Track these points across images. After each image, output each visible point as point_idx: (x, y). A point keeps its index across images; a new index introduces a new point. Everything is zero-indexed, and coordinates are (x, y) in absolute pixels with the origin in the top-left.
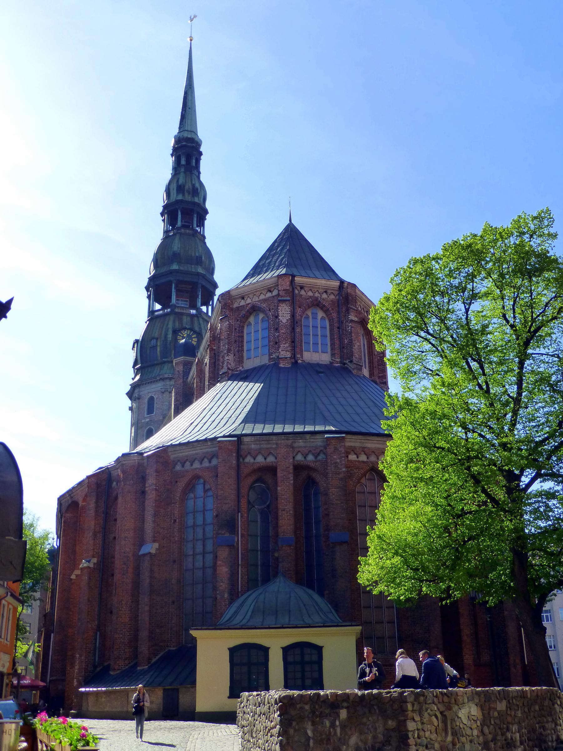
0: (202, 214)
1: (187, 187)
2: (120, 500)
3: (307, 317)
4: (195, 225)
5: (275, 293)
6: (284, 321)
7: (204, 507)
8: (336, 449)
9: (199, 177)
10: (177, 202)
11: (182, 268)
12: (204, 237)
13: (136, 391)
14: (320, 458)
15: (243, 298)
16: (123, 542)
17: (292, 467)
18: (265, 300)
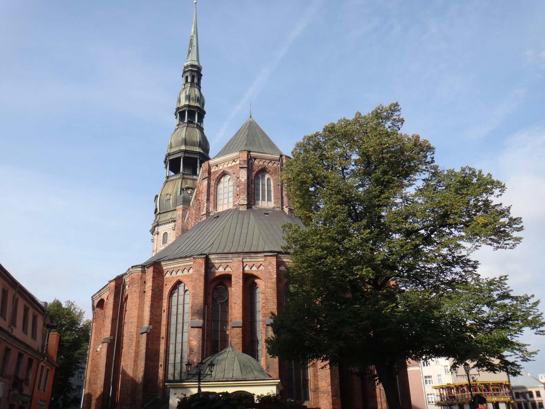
0: (202, 114)
1: (191, 97)
2: (129, 297)
3: (259, 179)
4: (196, 121)
5: (238, 162)
6: (243, 180)
7: (184, 302)
8: (270, 263)
9: (200, 90)
10: (185, 106)
11: (187, 149)
12: (203, 129)
13: (156, 228)
14: (260, 268)
15: (217, 166)
16: (130, 325)
17: (242, 275)
18: (231, 167)
